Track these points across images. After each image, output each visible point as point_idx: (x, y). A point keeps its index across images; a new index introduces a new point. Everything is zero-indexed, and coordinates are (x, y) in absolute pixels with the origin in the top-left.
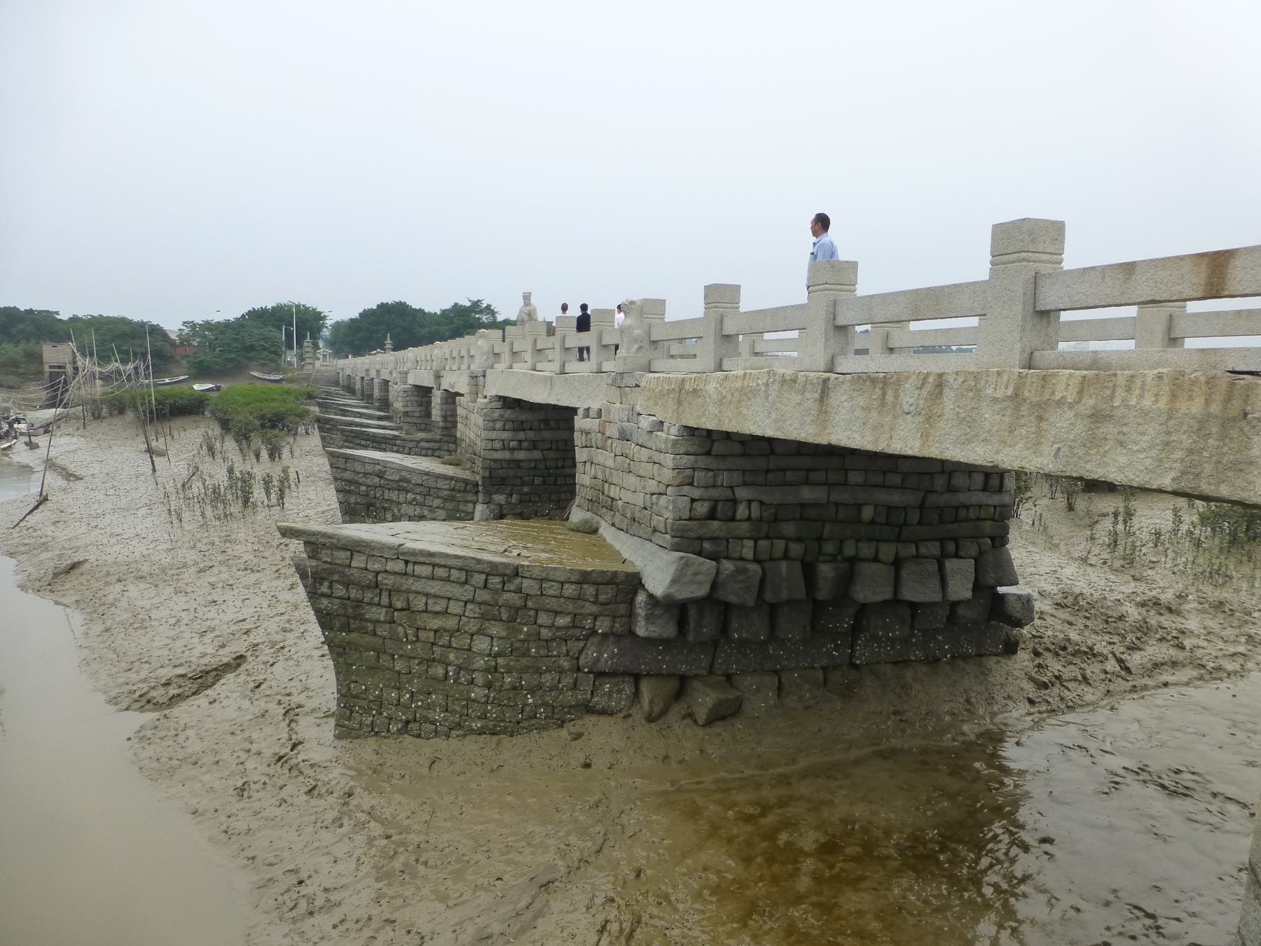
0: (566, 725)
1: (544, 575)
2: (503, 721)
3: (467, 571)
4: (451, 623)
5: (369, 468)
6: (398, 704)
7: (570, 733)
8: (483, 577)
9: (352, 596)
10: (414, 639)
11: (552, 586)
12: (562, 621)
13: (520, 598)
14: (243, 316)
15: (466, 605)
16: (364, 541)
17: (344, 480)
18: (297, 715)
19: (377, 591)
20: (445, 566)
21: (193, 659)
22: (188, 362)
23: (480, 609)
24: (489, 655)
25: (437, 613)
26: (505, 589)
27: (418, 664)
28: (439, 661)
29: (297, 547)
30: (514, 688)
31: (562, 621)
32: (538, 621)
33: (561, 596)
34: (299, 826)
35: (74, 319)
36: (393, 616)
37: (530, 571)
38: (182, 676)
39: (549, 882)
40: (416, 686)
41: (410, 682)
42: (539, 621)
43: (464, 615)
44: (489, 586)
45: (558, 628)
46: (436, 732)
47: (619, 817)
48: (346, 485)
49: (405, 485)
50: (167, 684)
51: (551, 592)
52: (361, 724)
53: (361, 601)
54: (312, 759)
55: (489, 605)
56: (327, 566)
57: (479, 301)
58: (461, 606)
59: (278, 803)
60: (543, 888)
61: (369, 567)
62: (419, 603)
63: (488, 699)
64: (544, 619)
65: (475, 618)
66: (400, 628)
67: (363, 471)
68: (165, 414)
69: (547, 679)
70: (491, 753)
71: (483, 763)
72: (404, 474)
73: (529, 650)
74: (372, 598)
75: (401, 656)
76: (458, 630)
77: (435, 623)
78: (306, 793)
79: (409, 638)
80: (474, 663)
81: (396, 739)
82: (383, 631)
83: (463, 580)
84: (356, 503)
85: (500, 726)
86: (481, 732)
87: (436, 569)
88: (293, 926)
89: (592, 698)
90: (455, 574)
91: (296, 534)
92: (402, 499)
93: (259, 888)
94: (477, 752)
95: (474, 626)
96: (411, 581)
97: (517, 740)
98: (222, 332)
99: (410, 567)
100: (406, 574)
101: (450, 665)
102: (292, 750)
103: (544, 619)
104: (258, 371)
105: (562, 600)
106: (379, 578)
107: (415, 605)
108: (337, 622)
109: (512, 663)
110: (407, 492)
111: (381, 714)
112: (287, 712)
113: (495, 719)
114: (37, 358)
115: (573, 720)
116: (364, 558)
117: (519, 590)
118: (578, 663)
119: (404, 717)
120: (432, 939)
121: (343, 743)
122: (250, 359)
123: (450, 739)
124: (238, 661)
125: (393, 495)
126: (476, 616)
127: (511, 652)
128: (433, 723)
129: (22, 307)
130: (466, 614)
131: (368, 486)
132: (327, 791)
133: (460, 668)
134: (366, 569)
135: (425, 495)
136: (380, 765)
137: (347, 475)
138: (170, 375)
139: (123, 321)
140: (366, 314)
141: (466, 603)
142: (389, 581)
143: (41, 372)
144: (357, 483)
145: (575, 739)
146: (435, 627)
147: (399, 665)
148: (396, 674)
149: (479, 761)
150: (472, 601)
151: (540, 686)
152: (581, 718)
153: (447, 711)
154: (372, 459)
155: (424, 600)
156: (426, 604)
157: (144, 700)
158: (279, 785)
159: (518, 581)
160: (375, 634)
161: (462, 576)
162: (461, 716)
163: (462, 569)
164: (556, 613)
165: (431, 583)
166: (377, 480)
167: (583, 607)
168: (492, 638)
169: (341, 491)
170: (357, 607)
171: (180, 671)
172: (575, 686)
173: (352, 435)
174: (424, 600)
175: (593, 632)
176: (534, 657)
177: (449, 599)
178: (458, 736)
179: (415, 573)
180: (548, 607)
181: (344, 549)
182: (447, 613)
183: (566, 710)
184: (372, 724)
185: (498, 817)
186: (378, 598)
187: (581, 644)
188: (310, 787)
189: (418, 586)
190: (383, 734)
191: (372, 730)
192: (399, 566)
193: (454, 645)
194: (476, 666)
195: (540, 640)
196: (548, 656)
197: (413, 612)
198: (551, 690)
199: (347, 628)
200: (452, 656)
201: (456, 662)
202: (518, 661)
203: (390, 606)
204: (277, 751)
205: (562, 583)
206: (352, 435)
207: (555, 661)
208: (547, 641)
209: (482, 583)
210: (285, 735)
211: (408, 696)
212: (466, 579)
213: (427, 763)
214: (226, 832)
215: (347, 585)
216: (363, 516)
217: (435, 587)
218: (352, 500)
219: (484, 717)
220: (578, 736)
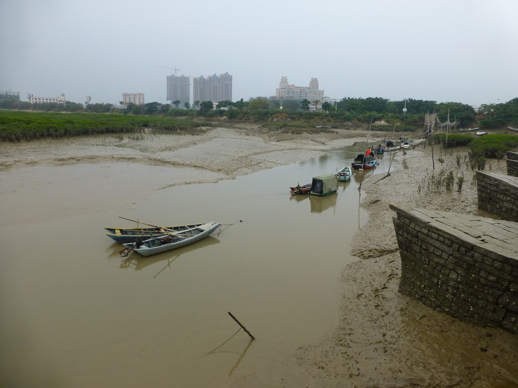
0: (487, 327)
1: (485, 253)
2: (458, 313)
3: (451, 241)
4: (442, 262)
5: (492, 182)
6: (420, 288)
7: (486, 332)
8: (458, 246)
9: (409, 238)
10: (428, 263)
11: (488, 260)
12: (491, 278)
13: (473, 261)
14: (510, 101)
15: (449, 256)
16: (415, 217)
17: (482, 186)
18: (393, 277)
19: (417, 239)
20: (443, 236)
21: (383, 245)
22: (480, 122)
23: (455, 260)
24: (456, 282)
25: (437, 255)
26: (467, 254)
27: (428, 274)
28: (436, 276)
29: (394, 214)
30: (464, 300)
31: (491, 278)
32: (480, 274)
33: (492, 266)
34: (365, 316)
35: (442, 104)
36: (421, 251)
37: (479, 250)
38: (376, 250)
39: (416, 384)
40: (426, 283)
41: (425, 280)
42: (481, 274)
43: (448, 260)
44: (460, 251)
45: (490, 281)
46: (431, 305)
47: (475, 380)
48: (482, 188)
49: (507, 193)
50: (370, 251)
51: (487, 262)
52: (406, 289)
53: (412, 241)
54: (385, 295)
55: (459, 259)
56: (402, 224)
58: (447, 256)
59: (365, 305)
60: (412, 385)
61: (415, 228)
62: (432, 249)
63: (453, 301)
64: (482, 274)
65: (452, 263)
66: (423, 257)
67: (490, 183)
68: (454, 145)
69: (481, 303)
70: (448, 324)
71: (441, 326)
72: (507, 187)
73: (474, 286)
74: (415, 241)
75: (423, 269)
76: (445, 266)
77: (437, 260)
78: (375, 306)
79: (426, 262)
80: (449, 283)
81: (416, 301)
82: (418, 256)
83: (449, 244)
84: (485, 197)
85: (456, 314)
86: (448, 313)
87: (440, 237)
88: (335, 346)
89: (503, 321)
90: (447, 241)
91: (394, 209)
92: (505, 199)
93: (340, 329)
94: (442, 321)
95: (451, 266)
96: (429, 239)
97: (462, 324)
98: (498, 109)
99: (430, 233)
100: (428, 235)
101: (440, 279)
102: (382, 289)
103: (482, 274)
104: (512, 126)
105: (493, 268)
106: (418, 234)
107: (430, 249)
108: (404, 247)
109: (465, 289)
110: (508, 196)
111: (413, 289)
112: (391, 275)
113: (455, 310)
114: (422, 119)
115: (491, 327)
116: (414, 224)
117: (472, 257)
118: (497, 301)
119: (421, 294)
120: (362, 376)
121: (400, 294)
122: (509, 121)
123: (435, 311)
124: (396, 251)
125: (501, 196)
126: (453, 262)
127: (466, 284)
128: (431, 301)
130: (449, 260)
131: (491, 190)
132: (381, 309)
133: (443, 283)
134: (415, 229)
135: (515, 199)
136: (406, 308)
137: (483, 184)
138: (472, 127)
139: (459, 105)
141: (449, 255)
142: (422, 236)
144: (486, 188)
145: (487, 336)
146: (436, 261)
147: (422, 272)
148: (420, 275)
149: (440, 325)
150: (452, 255)
151: (477, 304)
152: (496, 328)
153: (436, 298)
154: (494, 178)
155: (433, 248)
156: (434, 250)
157: (361, 254)
158: (370, 299)
159: (473, 252)
160: (415, 256)
161: (449, 243)
162: (441, 303)
163: (450, 240)
164: (490, 274)
165: (437, 242)
166: (495, 188)
167: (503, 275)
168: (458, 275)
169: (480, 190)
170: (410, 243)
171: (377, 248)
172: (494, 311)
173: (513, 164)
174: (433, 248)
175: (508, 289)
176: (476, 290)
177: (443, 251)
178: (438, 311)
179: (432, 236)
180: (485, 269)
181: (408, 219)
182: (441, 257)
183: (488, 321)
184: (410, 291)
185: (424, 349)
186: (417, 242)
187: (501, 293)
188: (377, 305)
189: (432, 241)
190: (413, 297)
191: (410, 294)
192: (425, 231)
193: (442, 271)
194: (450, 284)
195: (479, 283)
196: (482, 292)
197: (429, 252)
198: (482, 308)
199: (406, 250)
200: (441, 276)
201: (442, 279)
202: (468, 289)
203: (421, 247)
204: (378, 287)
205: (494, 260)
206: (513, 164)
207: (485, 296)
208: (483, 285)
209: (457, 249)
210: (384, 283)
211: (423, 286)
212: (451, 245)
213: (421, 316)
214: (346, 307)
215: (408, 233)
216: (487, 203)
217: (438, 244)
218: (483, 195)
219: (450, 307)
220: (489, 335)
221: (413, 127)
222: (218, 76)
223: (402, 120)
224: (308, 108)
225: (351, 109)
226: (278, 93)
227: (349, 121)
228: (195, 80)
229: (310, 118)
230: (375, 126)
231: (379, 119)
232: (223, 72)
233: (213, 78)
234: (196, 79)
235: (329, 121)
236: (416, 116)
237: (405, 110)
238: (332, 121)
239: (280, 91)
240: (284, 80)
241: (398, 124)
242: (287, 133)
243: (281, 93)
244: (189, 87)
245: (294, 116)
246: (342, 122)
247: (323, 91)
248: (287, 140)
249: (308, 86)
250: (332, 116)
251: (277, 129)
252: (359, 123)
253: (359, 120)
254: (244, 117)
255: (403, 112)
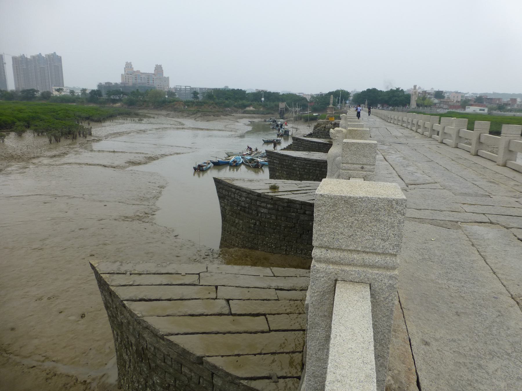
35: (283, 94)
57: (399, 88)
114: (278, 106)
129: (272, 92)
140: (363, 92)
143: (278, 110)
221: (273, 112)
222: (45, 57)
223: (264, 106)
224: (198, 98)
225: (229, 99)
226: (124, 78)
227: (228, 108)
228: (15, 59)
229: (201, 105)
230: (247, 111)
231: (249, 106)
232: (50, 52)
233: (38, 58)
234: (15, 58)
235: (215, 107)
236: (272, 104)
237: (263, 99)
238: (217, 107)
239: (126, 76)
240: (128, 66)
241: (261, 109)
242: (210, 116)
243: (127, 79)
244: (3, 67)
245: (189, 104)
246: (224, 108)
247: (168, 78)
248: (213, 120)
249: (153, 72)
250: (216, 104)
251: (194, 114)
252: (236, 109)
253: (235, 106)
254: (143, 104)
255: (261, 101)
